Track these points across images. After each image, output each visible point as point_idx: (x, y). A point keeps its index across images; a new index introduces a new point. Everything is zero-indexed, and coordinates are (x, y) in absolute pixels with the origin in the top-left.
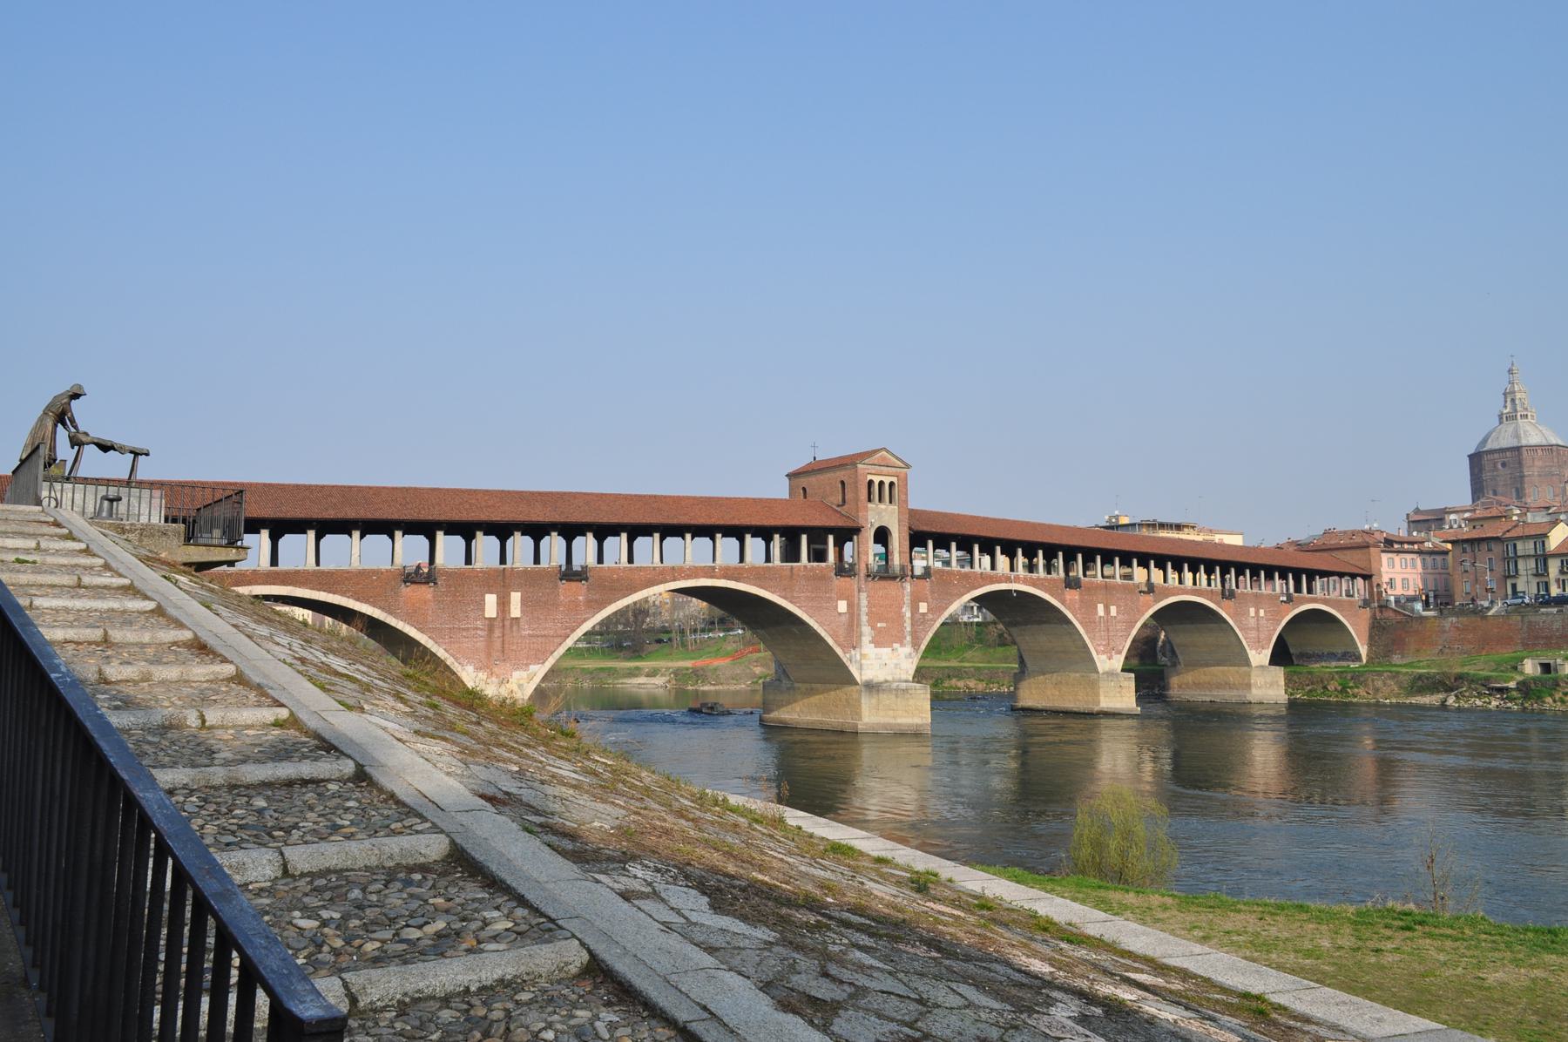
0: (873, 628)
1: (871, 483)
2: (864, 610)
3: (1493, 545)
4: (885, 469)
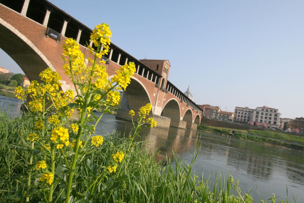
0: (158, 102)
1: (165, 67)
2: (158, 97)
3: (209, 110)
4: (167, 65)
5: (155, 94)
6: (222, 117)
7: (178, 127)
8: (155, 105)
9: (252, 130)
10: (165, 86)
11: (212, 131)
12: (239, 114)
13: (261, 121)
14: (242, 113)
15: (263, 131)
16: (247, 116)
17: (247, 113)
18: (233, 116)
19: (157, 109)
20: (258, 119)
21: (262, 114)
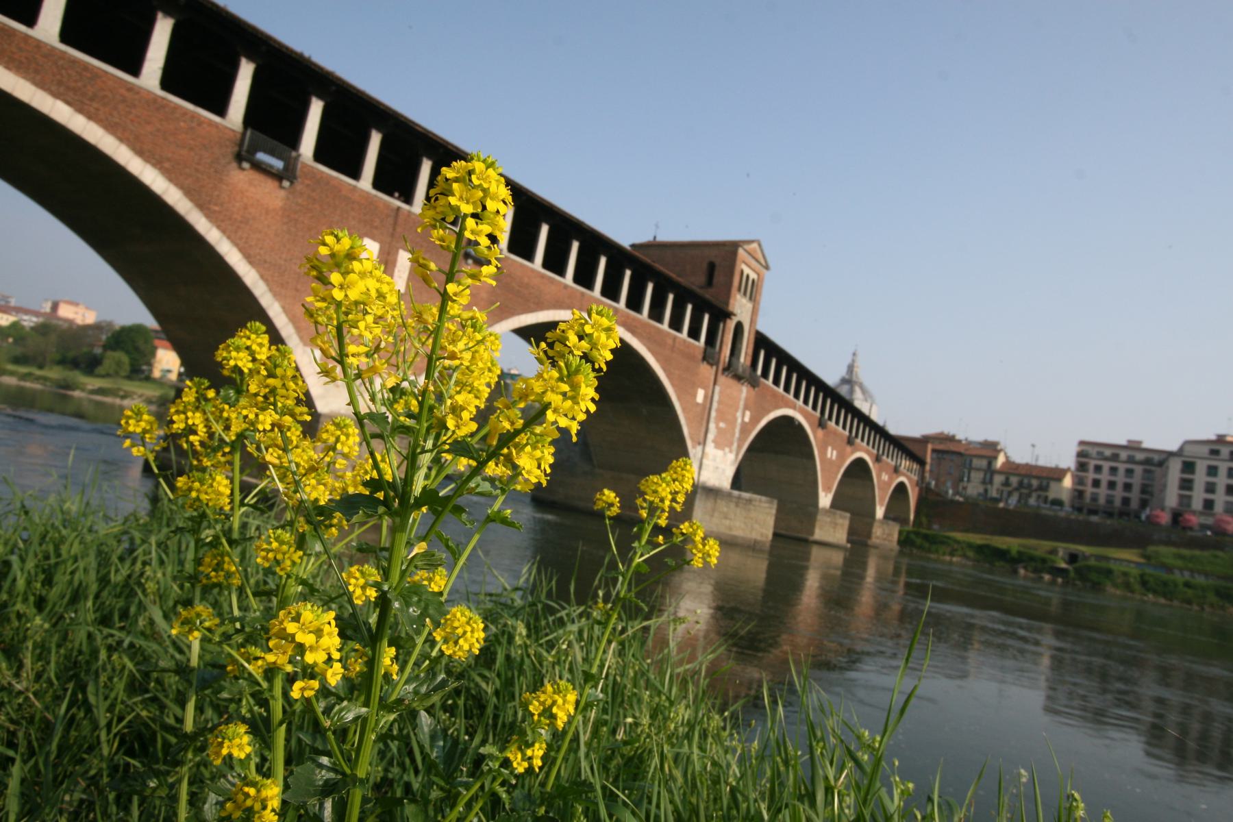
0: (717, 427)
1: (742, 272)
2: (715, 405)
5: (700, 395)
6: (1016, 489)
7: (812, 538)
8: (701, 440)
9: (1163, 549)
10: (744, 358)
11: (971, 554)
12: (1097, 476)
13: (1209, 504)
14: (1113, 470)
15: (1220, 554)
16: (1137, 481)
17: (1138, 469)
18: (1068, 482)
19: (714, 460)
20: (1190, 497)
21: (1212, 471)
